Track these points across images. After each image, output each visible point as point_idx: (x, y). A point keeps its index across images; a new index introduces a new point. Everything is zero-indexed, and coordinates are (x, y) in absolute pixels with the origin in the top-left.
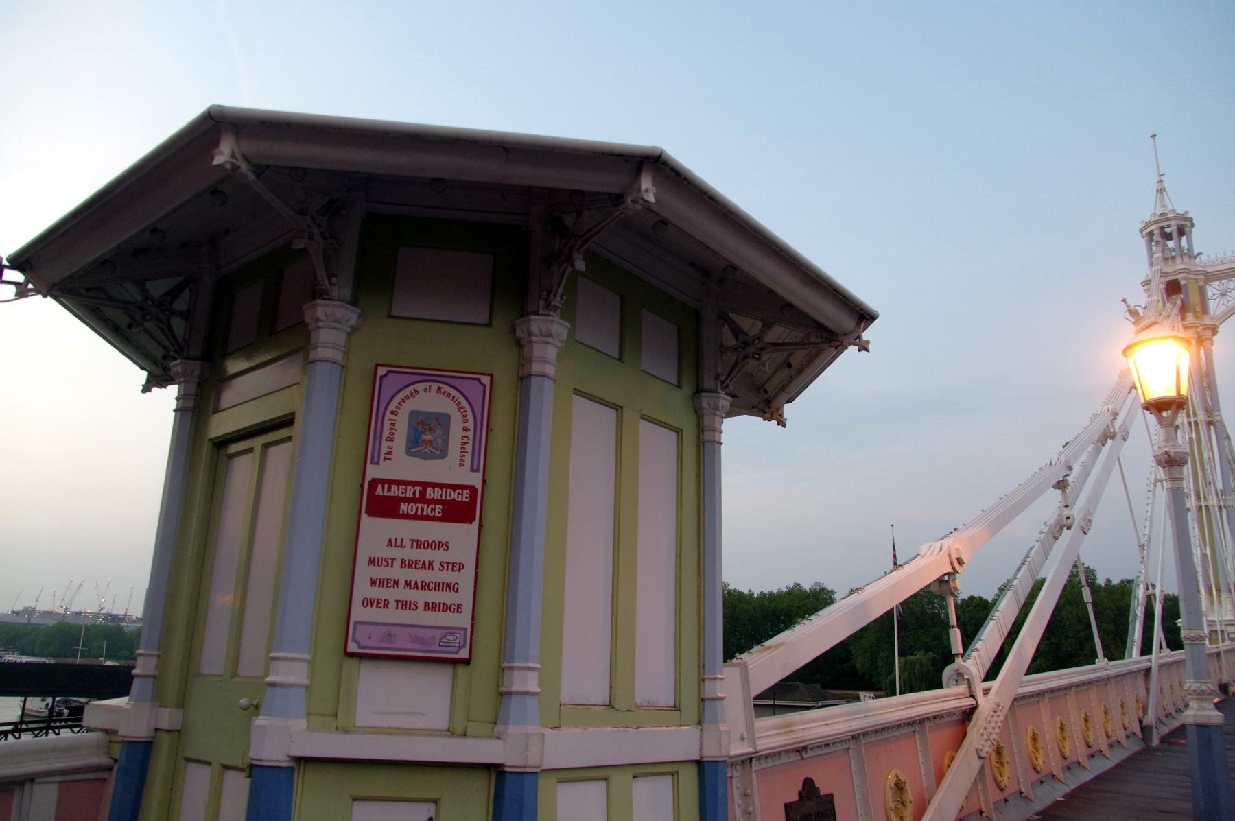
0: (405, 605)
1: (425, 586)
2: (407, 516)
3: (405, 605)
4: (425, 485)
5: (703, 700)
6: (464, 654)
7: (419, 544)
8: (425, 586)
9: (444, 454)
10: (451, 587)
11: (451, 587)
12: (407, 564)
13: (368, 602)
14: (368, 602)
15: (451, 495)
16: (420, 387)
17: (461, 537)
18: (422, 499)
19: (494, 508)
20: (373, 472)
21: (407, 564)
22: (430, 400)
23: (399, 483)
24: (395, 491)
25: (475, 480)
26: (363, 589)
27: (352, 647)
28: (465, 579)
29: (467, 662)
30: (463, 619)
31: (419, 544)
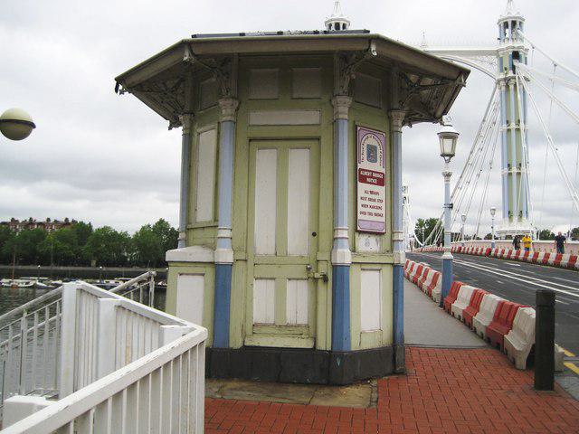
0: (370, 214)
1: (374, 207)
2: (369, 183)
3: (370, 214)
4: (373, 172)
5: (334, 239)
6: (384, 231)
7: (372, 192)
8: (374, 207)
9: (376, 161)
10: (380, 208)
11: (380, 208)
12: (370, 200)
13: (362, 213)
14: (362, 213)
15: (379, 176)
16: (369, 135)
17: (381, 190)
18: (371, 177)
19: (387, 181)
20: (359, 166)
21: (370, 200)
22: (372, 141)
23: (367, 171)
24: (366, 173)
25: (383, 171)
26: (360, 209)
27: (359, 229)
28: (383, 205)
29: (383, 234)
30: (383, 219)
31: (372, 192)
